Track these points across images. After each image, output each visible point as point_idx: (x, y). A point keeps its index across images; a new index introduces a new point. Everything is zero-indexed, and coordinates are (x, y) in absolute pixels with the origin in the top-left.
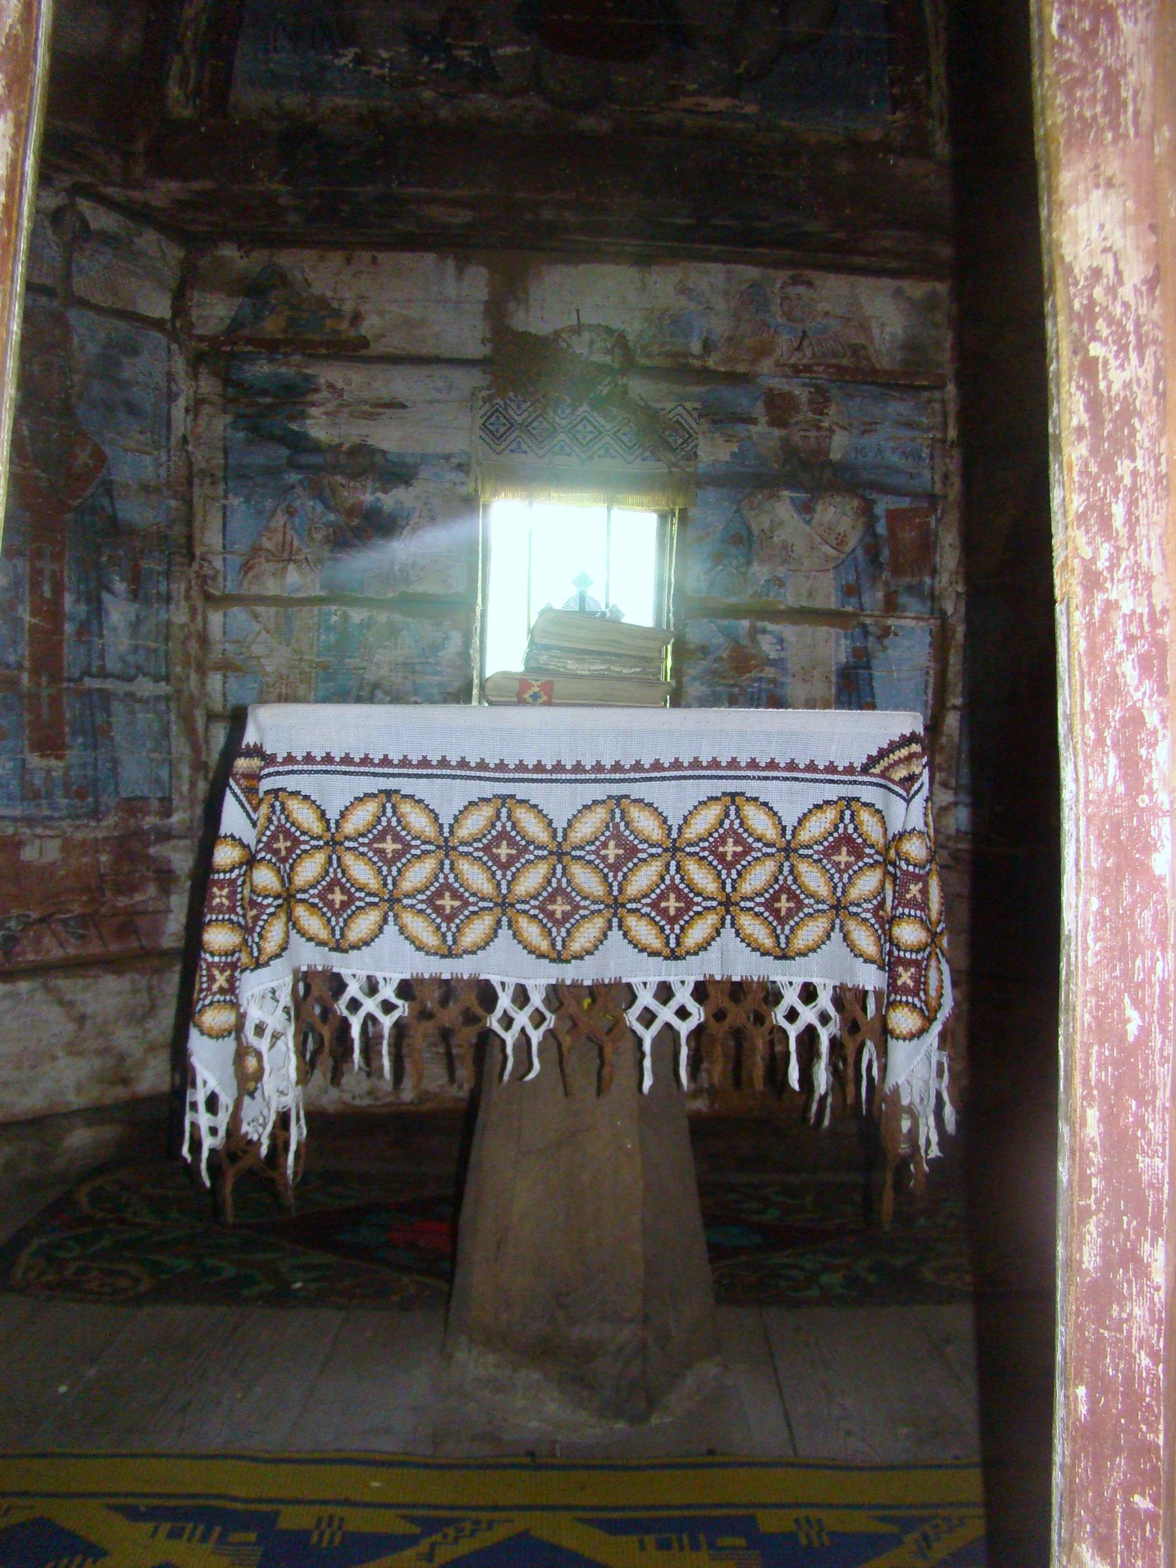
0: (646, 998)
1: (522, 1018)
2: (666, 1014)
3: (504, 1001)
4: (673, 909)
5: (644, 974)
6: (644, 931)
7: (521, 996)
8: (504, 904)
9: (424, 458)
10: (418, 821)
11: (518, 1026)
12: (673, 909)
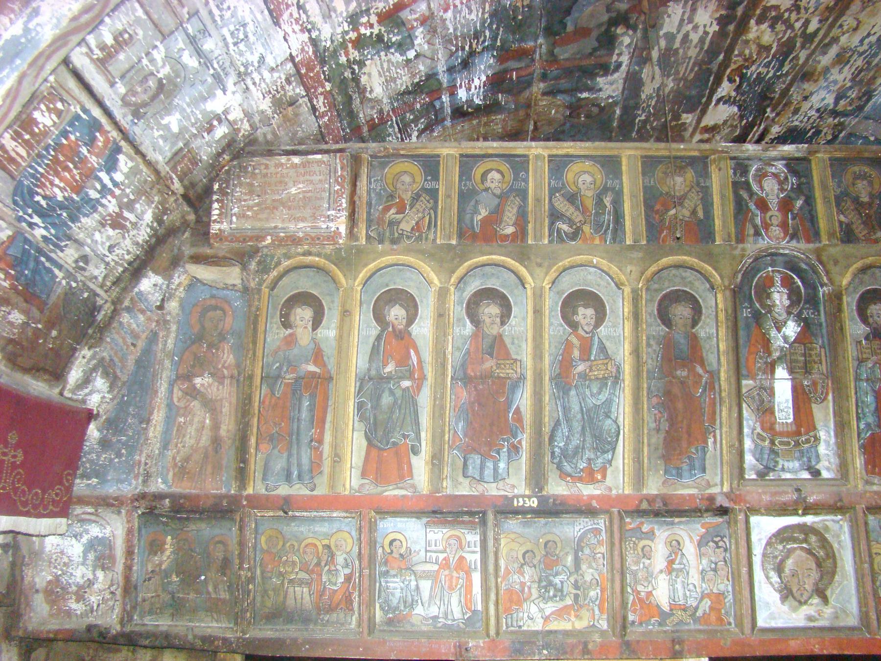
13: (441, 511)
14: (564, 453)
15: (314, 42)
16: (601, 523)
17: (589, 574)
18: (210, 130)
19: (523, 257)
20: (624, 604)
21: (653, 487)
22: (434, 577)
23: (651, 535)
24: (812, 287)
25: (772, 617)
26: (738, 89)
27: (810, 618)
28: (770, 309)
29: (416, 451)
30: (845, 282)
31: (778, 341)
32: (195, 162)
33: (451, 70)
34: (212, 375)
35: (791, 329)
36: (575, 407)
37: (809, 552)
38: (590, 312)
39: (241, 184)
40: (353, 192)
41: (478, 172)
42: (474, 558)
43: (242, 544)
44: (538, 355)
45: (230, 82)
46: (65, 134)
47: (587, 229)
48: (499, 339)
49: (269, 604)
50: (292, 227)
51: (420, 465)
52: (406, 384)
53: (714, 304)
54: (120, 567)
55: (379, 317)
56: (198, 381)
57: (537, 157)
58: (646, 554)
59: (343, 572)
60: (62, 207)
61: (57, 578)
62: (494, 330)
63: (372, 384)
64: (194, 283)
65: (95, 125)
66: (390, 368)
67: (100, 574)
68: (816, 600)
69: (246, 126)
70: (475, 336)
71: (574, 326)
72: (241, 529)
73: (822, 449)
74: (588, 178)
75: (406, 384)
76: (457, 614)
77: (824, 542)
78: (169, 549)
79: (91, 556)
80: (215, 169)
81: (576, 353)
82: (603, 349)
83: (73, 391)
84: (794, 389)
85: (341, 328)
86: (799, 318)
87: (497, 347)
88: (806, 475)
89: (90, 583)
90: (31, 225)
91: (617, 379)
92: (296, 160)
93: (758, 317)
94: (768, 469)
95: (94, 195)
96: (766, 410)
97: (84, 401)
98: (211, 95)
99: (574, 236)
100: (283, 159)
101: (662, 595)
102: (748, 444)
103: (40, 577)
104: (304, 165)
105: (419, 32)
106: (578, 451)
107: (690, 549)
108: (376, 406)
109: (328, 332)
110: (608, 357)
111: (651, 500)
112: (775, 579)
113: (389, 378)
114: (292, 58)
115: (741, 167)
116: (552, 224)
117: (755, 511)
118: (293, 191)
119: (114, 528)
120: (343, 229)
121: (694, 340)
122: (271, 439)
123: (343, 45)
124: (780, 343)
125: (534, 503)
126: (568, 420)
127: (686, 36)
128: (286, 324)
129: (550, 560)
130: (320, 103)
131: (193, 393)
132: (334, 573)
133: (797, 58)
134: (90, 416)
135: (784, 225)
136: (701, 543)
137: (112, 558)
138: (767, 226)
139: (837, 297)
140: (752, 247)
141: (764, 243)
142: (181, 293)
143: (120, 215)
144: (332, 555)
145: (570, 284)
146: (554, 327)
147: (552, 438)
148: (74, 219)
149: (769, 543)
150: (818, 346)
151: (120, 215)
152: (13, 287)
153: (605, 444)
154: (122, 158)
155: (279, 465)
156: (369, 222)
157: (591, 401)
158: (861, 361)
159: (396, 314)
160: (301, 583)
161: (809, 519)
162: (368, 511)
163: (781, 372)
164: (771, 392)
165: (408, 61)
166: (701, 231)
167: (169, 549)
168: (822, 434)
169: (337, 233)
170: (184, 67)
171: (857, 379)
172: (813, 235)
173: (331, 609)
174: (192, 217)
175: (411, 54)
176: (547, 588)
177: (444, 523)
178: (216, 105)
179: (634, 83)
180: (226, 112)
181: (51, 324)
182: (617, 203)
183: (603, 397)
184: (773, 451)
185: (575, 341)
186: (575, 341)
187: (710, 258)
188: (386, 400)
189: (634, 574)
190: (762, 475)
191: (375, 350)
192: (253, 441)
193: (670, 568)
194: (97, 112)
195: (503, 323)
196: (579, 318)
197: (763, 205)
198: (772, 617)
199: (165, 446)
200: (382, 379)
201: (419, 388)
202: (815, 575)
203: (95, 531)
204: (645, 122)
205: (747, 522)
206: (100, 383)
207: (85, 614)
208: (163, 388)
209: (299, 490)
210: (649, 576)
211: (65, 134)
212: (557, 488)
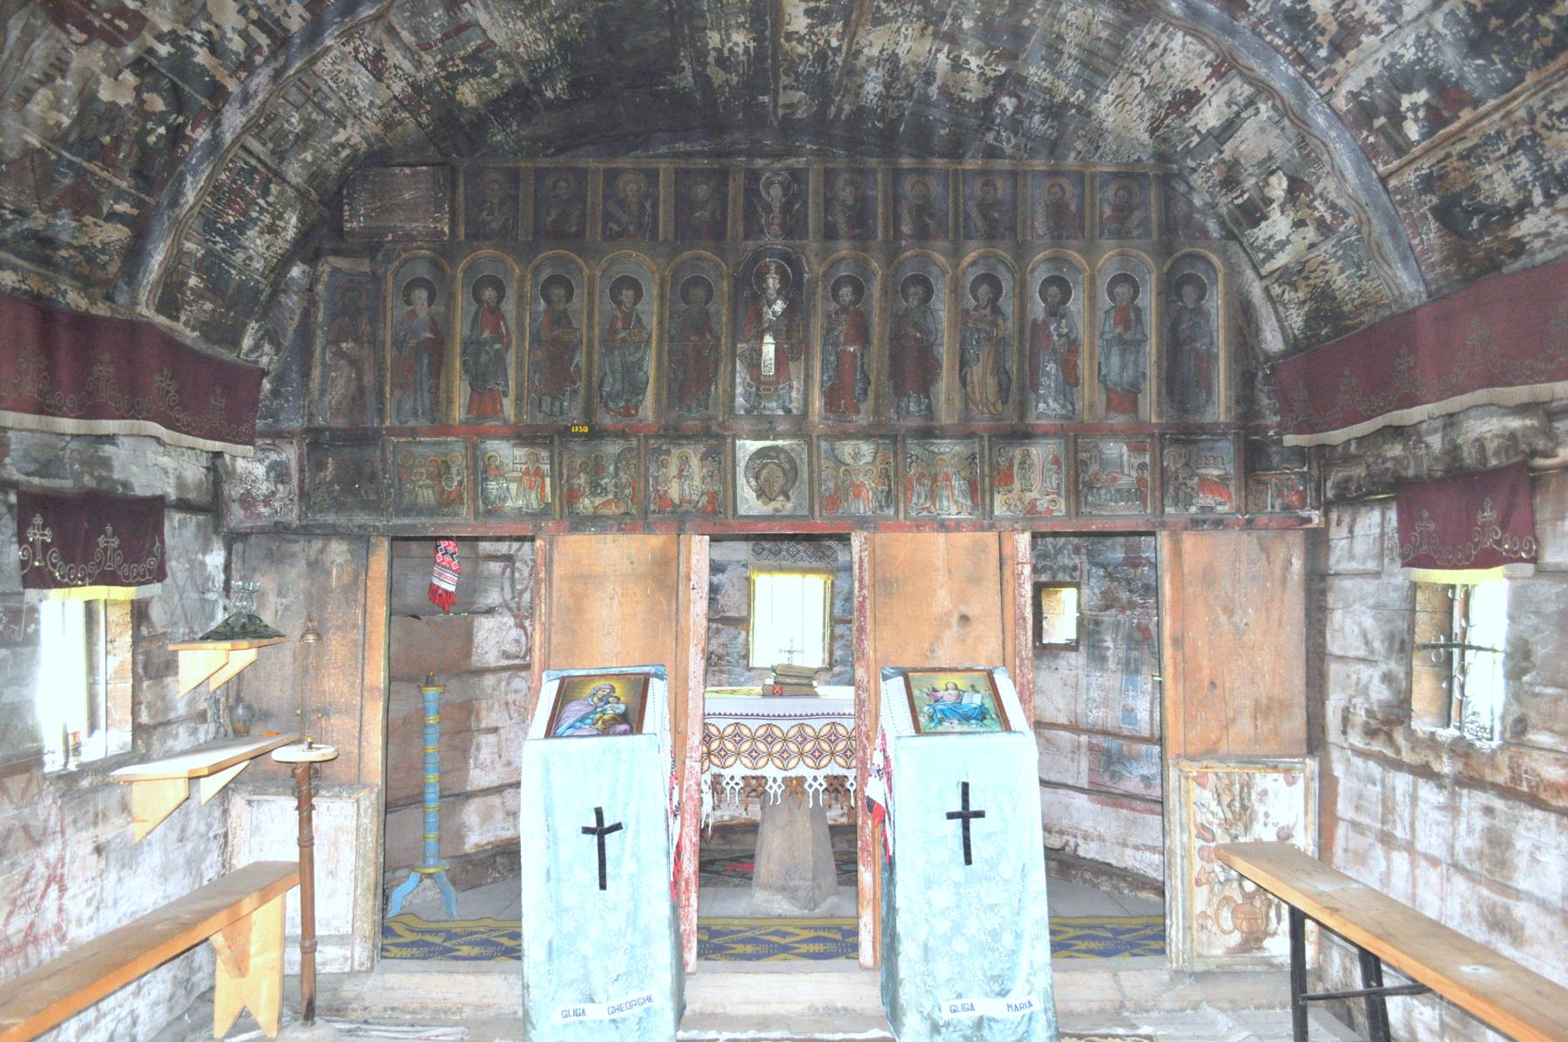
0: (810, 781)
1: (775, 787)
2: (816, 785)
3: (770, 782)
4: (817, 755)
5: (809, 773)
6: (809, 762)
7: (775, 780)
8: (770, 754)
9: (729, 562)
10: (745, 731)
11: (774, 789)
12: (817, 755)
13: (523, 436)
14: (609, 395)
15: (412, 85)
17: (624, 478)
18: (337, 153)
20: (647, 497)
22: (519, 480)
23: (668, 452)
25: (750, 508)
26: (796, 80)
27: (776, 510)
28: (764, 290)
29: (505, 395)
32: (326, 176)
33: (533, 80)
34: (355, 341)
35: (779, 306)
37: (778, 465)
38: (630, 293)
39: (364, 190)
40: (453, 200)
41: (549, 182)
42: (546, 468)
43: (384, 461)
44: (590, 327)
45: (349, 122)
46: (234, 181)
47: (631, 228)
49: (406, 501)
50: (407, 226)
51: (508, 405)
52: (497, 346)
54: (295, 481)
55: (478, 299)
56: (344, 345)
57: (597, 169)
58: (664, 465)
59: (457, 479)
60: (234, 227)
61: (248, 491)
63: (473, 346)
64: (335, 271)
65: (254, 170)
66: (486, 334)
67: (280, 487)
68: (781, 498)
69: (365, 145)
70: (546, 311)
71: (619, 303)
72: (383, 450)
74: (633, 186)
75: (497, 346)
76: (535, 506)
77: (792, 461)
78: (331, 467)
79: (272, 474)
80: (344, 180)
81: (620, 324)
82: (639, 320)
83: (246, 355)
84: (776, 351)
85: (448, 307)
86: (786, 299)
88: (780, 412)
89: (273, 493)
90: (215, 243)
91: (648, 342)
92: (407, 171)
95: (254, 215)
96: (754, 363)
97: (257, 362)
98: (335, 132)
99: (620, 234)
100: (397, 170)
101: (674, 493)
102: (739, 390)
103: (233, 491)
104: (414, 174)
105: (499, 65)
108: (476, 362)
110: (642, 326)
112: (753, 483)
113: (486, 342)
114: (395, 97)
115: (754, 176)
116: (605, 225)
117: (740, 437)
118: (407, 196)
119: (290, 454)
120: (446, 229)
122: (401, 386)
123: (436, 80)
124: (770, 316)
125: (586, 430)
126: (613, 372)
127: (731, 50)
128: (408, 302)
130: (424, 119)
131: (340, 354)
132: (449, 479)
133: (833, 62)
134: (264, 373)
135: (783, 225)
136: (702, 459)
137: (289, 475)
138: (769, 225)
142: (325, 278)
143: (273, 224)
144: (448, 468)
145: (617, 272)
146: (605, 305)
147: (601, 385)
148: (242, 233)
149: (751, 459)
151: (273, 224)
152: (206, 287)
153: (637, 389)
154: (272, 186)
155: (407, 406)
156: (467, 223)
160: (427, 487)
161: (780, 443)
163: (768, 339)
165: (494, 81)
166: (717, 232)
167: (331, 467)
168: (795, 384)
169: (442, 232)
170: (315, 122)
171: (825, 344)
173: (448, 505)
174: (327, 214)
175: (496, 76)
176: (595, 488)
178: (341, 136)
179: (703, 80)
180: (348, 139)
181: (229, 308)
182: (655, 206)
183: (638, 356)
184: (758, 395)
185: (618, 314)
186: (618, 314)
187: (720, 252)
188: (484, 358)
189: (656, 479)
190: (748, 412)
191: (475, 321)
192: (388, 389)
193: (680, 476)
194: (254, 162)
195: (568, 301)
196: (622, 297)
197: (768, 208)
198: (750, 508)
199: (323, 393)
200: (479, 344)
201: (507, 349)
202: (781, 481)
203: (274, 456)
204: (727, 101)
205: (734, 444)
206: (267, 348)
207: (272, 515)
208: (318, 350)
210: (667, 481)
211: (234, 181)
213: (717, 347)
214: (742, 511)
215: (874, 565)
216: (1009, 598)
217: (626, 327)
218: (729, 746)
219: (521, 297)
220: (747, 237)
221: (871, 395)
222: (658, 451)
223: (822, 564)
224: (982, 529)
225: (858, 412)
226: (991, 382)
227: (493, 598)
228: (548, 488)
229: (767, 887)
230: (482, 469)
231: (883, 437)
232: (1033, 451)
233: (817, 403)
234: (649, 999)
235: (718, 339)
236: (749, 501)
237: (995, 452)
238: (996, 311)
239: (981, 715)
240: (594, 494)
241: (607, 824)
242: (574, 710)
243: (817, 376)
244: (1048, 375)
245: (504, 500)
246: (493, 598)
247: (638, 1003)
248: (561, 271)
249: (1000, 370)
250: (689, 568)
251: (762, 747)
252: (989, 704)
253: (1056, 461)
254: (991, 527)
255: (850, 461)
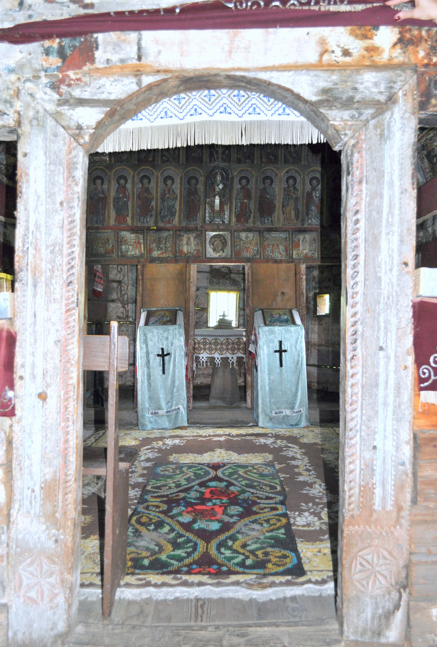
5: (230, 356)
11: (218, 361)
12: (233, 349)
13: (134, 230)
14: (163, 216)
16: (171, 232)
17: (168, 245)
19: (154, 167)
20: (176, 251)
21: (184, 224)
22: (133, 245)
23: (183, 236)
24: (227, 175)
28: (216, 181)
30: (236, 174)
31: (217, 189)
35: (221, 186)
36: (166, 205)
44: (157, 192)
47: (171, 159)
48: (148, 188)
51: (129, 220)
53: (202, 179)
55: (118, 183)
58: (182, 240)
62: (147, 186)
63: (117, 200)
66: (121, 195)
70: (142, 188)
73: (226, 216)
77: (225, 239)
82: (173, 191)
87: (147, 190)
93: (213, 183)
94: (212, 221)
96: (212, 206)
101: (185, 249)
102: (207, 215)
106: (167, 216)
107: (192, 239)
109: (105, 186)
111: (182, 227)
121: (196, 188)
128: (95, 184)
129: (159, 241)
135: (222, 159)
136: (195, 238)
138: (218, 158)
139: (233, 178)
140: (212, 165)
141: (216, 163)
145: (166, 174)
146: (161, 185)
150: (227, 191)
153: (173, 214)
155: (95, 219)
157: (170, 204)
158: (238, 195)
159: (122, 181)
161: (221, 233)
162: (117, 230)
163: (217, 197)
164: (214, 202)
171: (236, 199)
172: (229, 161)
173: (109, 253)
176: (159, 248)
177: (134, 233)
190: (210, 222)
191: (117, 191)
193: (187, 244)
201: (128, 200)
202: (221, 246)
209: (100, 225)
210: (182, 245)
212: (161, 224)
213: (199, 201)
214: (208, 256)
215: (252, 275)
216: (298, 287)
217: (169, 193)
218: (202, 346)
219: (133, 182)
220: (210, 163)
221: (252, 216)
222: (180, 236)
223: (235, 288)
224: (289, 262)
225: (247, 222)
226: (293, 213)
227: (114, 296)
228: (142, 248)
229: (214, 398)
230: (120, 241)
231: (256, 231)
232: (307, 236)
233: (234, 219)
234: (179, 409)
235: (200, 197)
236: (210, 252)
237: (294, 236)
238: (295, 188)
239: (287, 321)
240: (158, 250)
241: (165, 353)
242: (152, 320)
243: (234, 210)
244: (312, 210)
245: (127, 252)
246: (114, 296)
247: (175, 410)
248: (147, 174)
249: (296, 210)
250: (190, 275)
251: (213, 347)
252: (290, 318)
253: (314, 240)
254: (292, 262)
255: (244, 239)
